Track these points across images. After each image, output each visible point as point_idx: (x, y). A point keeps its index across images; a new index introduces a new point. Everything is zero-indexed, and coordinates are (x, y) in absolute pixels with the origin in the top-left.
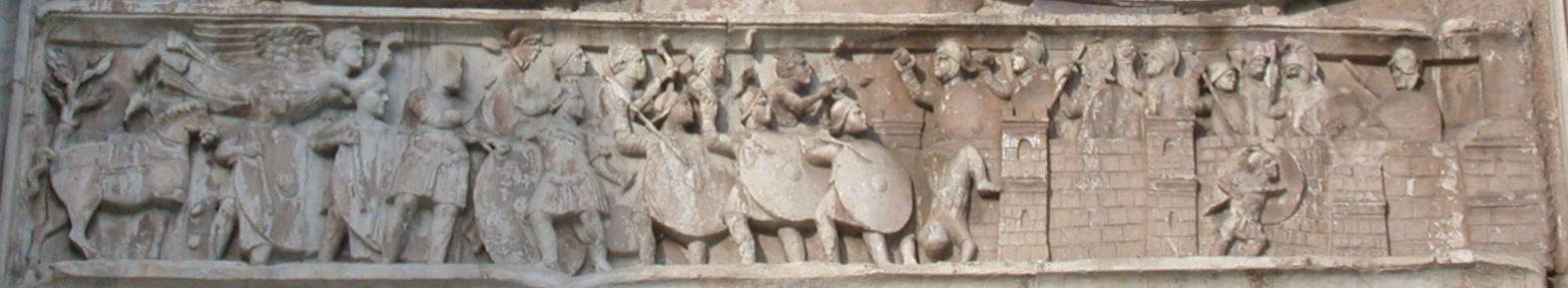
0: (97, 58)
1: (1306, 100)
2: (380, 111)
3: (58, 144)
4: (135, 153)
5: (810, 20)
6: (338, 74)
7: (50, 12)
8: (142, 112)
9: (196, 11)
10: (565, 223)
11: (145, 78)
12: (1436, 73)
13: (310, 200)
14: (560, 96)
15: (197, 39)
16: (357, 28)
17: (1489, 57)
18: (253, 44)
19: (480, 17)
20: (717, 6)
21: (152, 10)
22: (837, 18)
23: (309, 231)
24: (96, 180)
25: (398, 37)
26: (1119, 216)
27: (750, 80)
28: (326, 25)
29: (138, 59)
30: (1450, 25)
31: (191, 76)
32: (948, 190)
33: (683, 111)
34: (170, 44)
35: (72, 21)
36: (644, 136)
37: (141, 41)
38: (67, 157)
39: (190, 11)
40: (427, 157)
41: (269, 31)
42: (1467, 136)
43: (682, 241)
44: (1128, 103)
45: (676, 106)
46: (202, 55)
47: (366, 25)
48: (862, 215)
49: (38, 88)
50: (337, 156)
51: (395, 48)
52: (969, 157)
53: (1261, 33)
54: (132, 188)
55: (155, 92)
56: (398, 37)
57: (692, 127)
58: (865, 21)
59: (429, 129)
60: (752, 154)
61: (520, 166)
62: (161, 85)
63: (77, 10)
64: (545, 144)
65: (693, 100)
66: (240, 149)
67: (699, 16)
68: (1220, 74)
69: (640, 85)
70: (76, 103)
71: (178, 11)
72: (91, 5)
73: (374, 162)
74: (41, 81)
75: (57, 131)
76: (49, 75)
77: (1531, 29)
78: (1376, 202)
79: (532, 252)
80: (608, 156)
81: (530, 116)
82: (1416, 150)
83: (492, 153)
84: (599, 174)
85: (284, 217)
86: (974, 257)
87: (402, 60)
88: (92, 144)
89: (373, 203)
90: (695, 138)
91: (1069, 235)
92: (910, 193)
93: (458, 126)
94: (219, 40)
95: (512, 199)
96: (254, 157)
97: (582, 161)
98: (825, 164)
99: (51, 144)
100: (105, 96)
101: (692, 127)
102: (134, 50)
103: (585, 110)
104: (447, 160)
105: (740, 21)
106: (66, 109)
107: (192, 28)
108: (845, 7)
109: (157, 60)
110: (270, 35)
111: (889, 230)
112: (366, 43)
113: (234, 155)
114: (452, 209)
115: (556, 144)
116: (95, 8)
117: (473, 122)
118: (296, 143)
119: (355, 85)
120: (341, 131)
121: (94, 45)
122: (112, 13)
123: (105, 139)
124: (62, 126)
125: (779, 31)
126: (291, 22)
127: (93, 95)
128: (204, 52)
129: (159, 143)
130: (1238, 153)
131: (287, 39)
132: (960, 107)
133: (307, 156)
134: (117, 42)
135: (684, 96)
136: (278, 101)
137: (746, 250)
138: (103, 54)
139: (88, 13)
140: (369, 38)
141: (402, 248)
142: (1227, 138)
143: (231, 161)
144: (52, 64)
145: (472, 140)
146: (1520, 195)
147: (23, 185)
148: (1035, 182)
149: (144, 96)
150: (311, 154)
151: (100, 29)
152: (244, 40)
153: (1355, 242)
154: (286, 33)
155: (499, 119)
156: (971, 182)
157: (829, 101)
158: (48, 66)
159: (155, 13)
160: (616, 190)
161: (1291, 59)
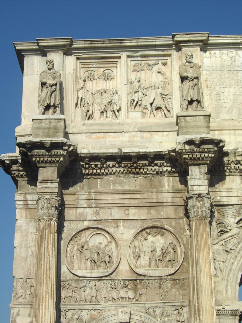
1: (169, 285)
6: (85, 284)
12: (180, 282)
13: (83, 296)
17: (185, 281)
22: (128, 278)
23: (83, 299)
24: (65, 295)
25: (90, 281)
26: (152, 296)
27: (121, 284)
28: (84, 280)
30: (181, 278)
32: (138, 294)
33: (115, 287)
42: (183, 288)
44: (154, 285)
48: (130, 297)
51: (90, 281)
52: (140, 291)
53: (165, 279)
54: (68, 295)
56: (90, 281)
67: (116, 278)
68: (161, 283)
77: (188, 278)
78: (174, 295)
79: (102, 300)
82: (178, 289)
85: (81, 297)
86: (140, 301)
89: (88, 296)
91: (148, 298)
108: (129, 277)
125: (123, 280)
127: (64, 286)
130: (163, 290)
132: (139, 286)
140: (88, 280)
142: (162, 289)
146: (187, 294)
155: (99, 288)
156: (140, 293)
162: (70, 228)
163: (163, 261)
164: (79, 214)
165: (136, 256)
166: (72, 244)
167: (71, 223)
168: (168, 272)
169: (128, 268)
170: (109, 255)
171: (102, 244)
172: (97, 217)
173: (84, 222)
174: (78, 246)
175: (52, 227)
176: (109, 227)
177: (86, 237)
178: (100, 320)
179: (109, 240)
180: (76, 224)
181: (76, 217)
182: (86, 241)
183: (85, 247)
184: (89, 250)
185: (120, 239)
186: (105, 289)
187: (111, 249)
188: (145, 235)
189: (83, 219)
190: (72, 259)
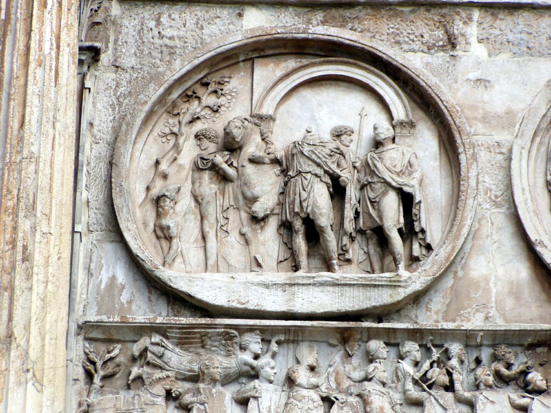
0: (112, 348)
3: (92, 395)
4: (136, 401)
5: (513, 328)
6: (247, 357)
7: (86, 322)
8: (139, 378)
9: (168, 322)
11: (139, 360)
14: (373, 371)
15: (167, 338)
16: (258, 332)
18: (200, 340)
19: (328, 325)
20: (459, 320)
21: (143, 321)
25: (282, 338)
29: (136, 349)
31: (165, 359)
34: (153, 340)
37: (136, 339)
38: (99, 403)
39: (165, 322)
40: (300, 405)
41: (209, 333)
45: (439, 376)
46: (171, 346)
47: (263, 330)
49: (80, 365)
50: (249, 404)
55: (145, 367)
56: (282, 338)
57: (450, 388)
58: (544, 328)
59: (301, 389)
60: (483, 403)
61: (352, 410)
62: (148, 363)
63: (100, 320)
64: (366, 397)
65: (450, 374)
66: (195, 399)
67: (450, 326)
70: (101, 373)
71: (157, 321)
72: (109, 318)
73: (270, 407)
74: (81, 361)
75: (91, 389)
76: (86, 358)
80: (401, 405)
81: (356, 382)
83: (337, 402)
88: (111, 396)
90: (450, 395)
93: (316, 387)
94: (180, 338)
96: (202, 404)
99: (88, 396)
100: (117, 369)
101: (450, 388)
102: (131, 344)
104: (311, 406)
105: (474, 329)
106: (96, 376)
107: (166, 331)
109: (146, 350)
110: (209, 335)
113: (192, 403)
115: (372, 398)
116: (111, 320)
117: (325, 384)
118: (225, 395)
121: (110, 341)
122: (120, 323)
123: (118, 393)
124: (95, 386)
126: (221, 328)
128: (172, 345)
129: (149, 395)
131: (219, 338)
133: (232, 404)
134: (123, 339)
135: (444, 371)
136: (217, 372)
138: (115, 346)
139: (107, 322)
143: (189, 407)
144: (87, 351)
145: (324, 395)
149: (139, 369)
150: (234, 403)
151: (113, 332)
152: (194, 338)
154: (219, 334)
155: (338, 384)
157: (525, 373)
158: (85, 353)
159: (145, 323)
162: (158, 41)
166: (167, 131)
170: (406, 189)
171: (354, 137)
173: (240, 15)
174: (206, 143)
176: (398, 43)
177: (255, 98)
184: (277, 169)
185: (468, 113)
190: (166, 214)
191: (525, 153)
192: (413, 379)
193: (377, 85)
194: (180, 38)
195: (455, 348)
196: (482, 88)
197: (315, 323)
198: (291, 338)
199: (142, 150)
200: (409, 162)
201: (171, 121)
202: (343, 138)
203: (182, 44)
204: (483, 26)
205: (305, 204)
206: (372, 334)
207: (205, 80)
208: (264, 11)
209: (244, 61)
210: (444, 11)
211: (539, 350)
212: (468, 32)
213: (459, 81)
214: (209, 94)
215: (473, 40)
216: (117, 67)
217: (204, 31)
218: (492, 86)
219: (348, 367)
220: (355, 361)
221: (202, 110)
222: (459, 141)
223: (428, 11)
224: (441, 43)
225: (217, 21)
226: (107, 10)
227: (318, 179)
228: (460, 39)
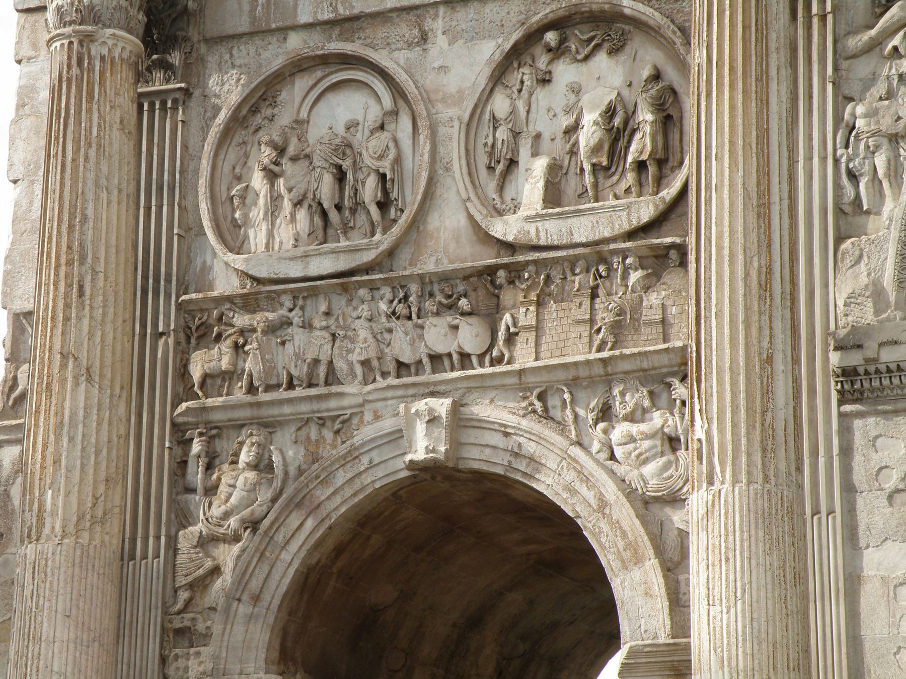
2: (301, 324)
6: (283, 312)
10: (365, 363)
28: (278, 293)
33: (405, 312)
35: (190, 302)
36: (394, 324)
40: (316, 342)
43: (407, 366)
47: (292, 291)
48: (468, 349)
57: (410, 318)
62: (225, 323)
65: (410, 307)
69: (392, 302)
70: (195, 335)
73: (299, 345)
84: (378, 340)
87: (309, 302)
90: (410, 322)
92: (489, 334)
93: (326, 328)
95: (347, 355)
97: (370, 336)
98: (456, 327)
101: (410, 318)
103: (371, 315)
104: (323, 343)
111: (479, 353)
112: (294, 297)
114: (326, 362)
119: (291, 315)
120: (286, 335)
124: (191, 345)
137: (428, 368)
141: (311, 379)
147: (178, 371)
148: (531, 327)
153: (650, 338)
156: (508, 328)
160: (384, 346)
161: (628, 261)
163: (613, 169)
164: (263, 5)
165: (499, 162)
166: (241, 141)
167: (232, 47)
168: (629, 215)
169: (463, 220)
170: (381, 170)
171: (360, 127)
172: (335, 9)
173: (285, 39)
175: (97, 68)
176: (388, 44)
178: (337, 460)
179: (387, 101)
180: (252, 51)
181: (253, 19)
182: (297, 122)
183: (291, 150)
186: (367, 324)
187: (391, 145)
188: (542, 61)
189: (280, 24)
191: (464, 127)
192: (387, 314)
193: (373, 83)
194: (245, 65)
195: (414, 288)
196: (443, 73)
197: (322, 282)
198: (312, 293)
199: (224, 160)
200: (387, 146)
201: (243, 133)
202: (351, 129)
203: (246, 70)
204: (445, 20)
205: (316, 193)
206: (361, 284)
207: (263, 97)
208: (301, 33)
209: (289, 76)
210: (419, 12)
211: (472, 279)
212: (435, 28)
213: (428, 70)
214: (267, 107)
215: (439, 33)
216: (205, 96)
217: (261, 57)
218: (449, 71)
219: (350, 308)
220: (354, 303)
221: (263, 120)
222: (419, 124)
223: (408, 14)
224: (416, 40)
225: (270, 47)
226: (198, 50)
227: (325, 171)
228: (429, 34)
